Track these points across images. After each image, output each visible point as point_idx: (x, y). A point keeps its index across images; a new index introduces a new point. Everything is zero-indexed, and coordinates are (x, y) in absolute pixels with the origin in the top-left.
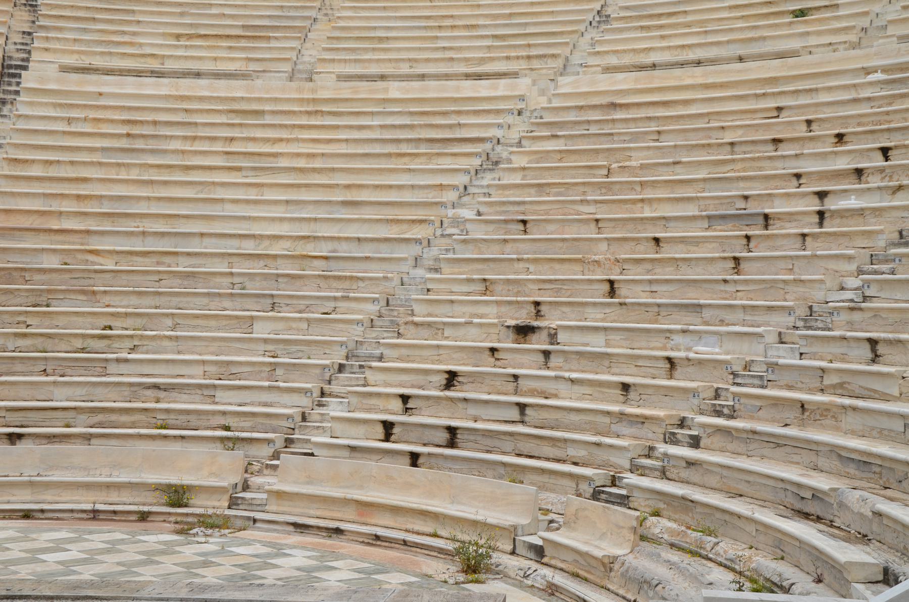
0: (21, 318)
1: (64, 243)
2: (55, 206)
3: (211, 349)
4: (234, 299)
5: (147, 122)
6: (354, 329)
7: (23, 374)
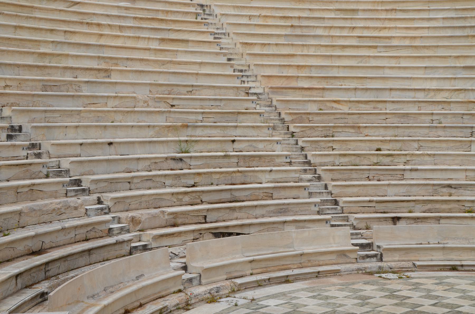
0: (330, 145)
1: (311, 96)
3: (457, 162)
4: (445, 129)
5: (295, 17)
7: (357, 180)
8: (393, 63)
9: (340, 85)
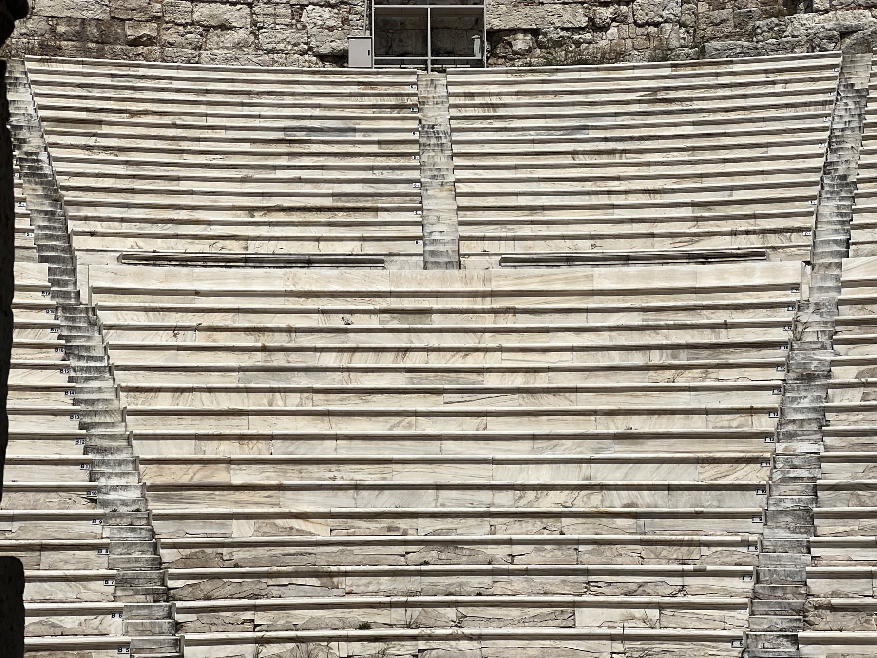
2: (212, 450)
6: (734, 618)
8: (470, 426)
9: (330, 478)
